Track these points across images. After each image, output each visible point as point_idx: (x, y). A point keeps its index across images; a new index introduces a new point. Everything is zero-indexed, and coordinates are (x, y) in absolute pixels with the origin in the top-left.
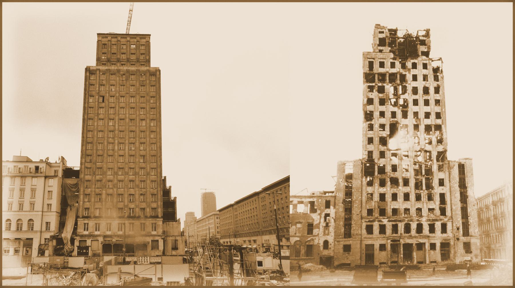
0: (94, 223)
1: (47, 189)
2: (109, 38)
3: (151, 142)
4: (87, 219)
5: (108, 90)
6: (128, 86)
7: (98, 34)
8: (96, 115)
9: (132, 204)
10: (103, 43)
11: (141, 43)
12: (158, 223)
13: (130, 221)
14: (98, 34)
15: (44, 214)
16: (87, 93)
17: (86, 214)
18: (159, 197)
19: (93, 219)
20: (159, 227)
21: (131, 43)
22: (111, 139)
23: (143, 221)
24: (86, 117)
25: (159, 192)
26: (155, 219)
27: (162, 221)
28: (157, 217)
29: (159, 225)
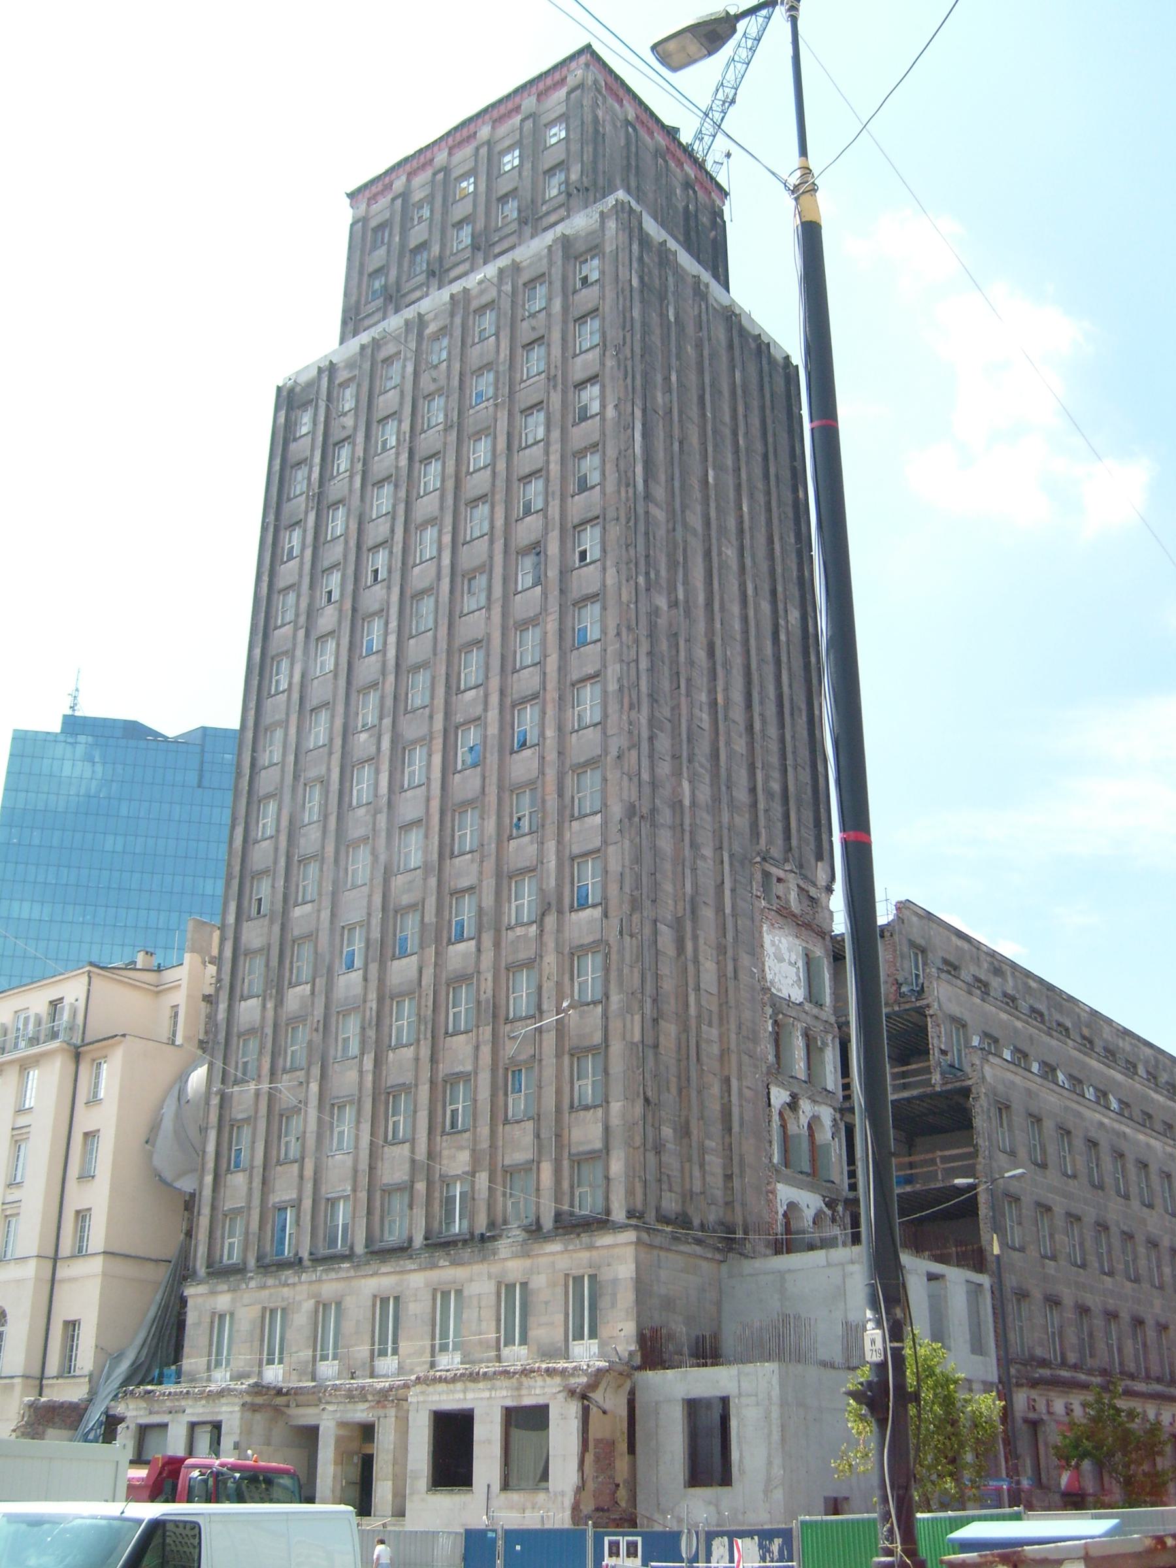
0: (254, 1312)
1: (85, 1121)
2: (399, 184)
3: (575, 676)
4: (225, 1287)
5: (361, 455)
6: (455, 382)
7: (351, 196)
8: (302, 619)
9: (461, 1148)
10: (373, 223)
11: (545, 119)
12: (606, 1275)
13: (434, 1275)
14: (351, 196)
15: (63, 1272)
16: (271, 518)
17: (230, 1257)
18: (617, 1066)
19: (253, 1284)
20: (613, 1305)
21: (499, 148)
22: (363, 736)
23: (515, 1268)
24: (258, 651)
25: (615, 1025)
26: (585, 1238)
27: (630, 1252)
28: (600, 1223)
29: (615, 1281)
